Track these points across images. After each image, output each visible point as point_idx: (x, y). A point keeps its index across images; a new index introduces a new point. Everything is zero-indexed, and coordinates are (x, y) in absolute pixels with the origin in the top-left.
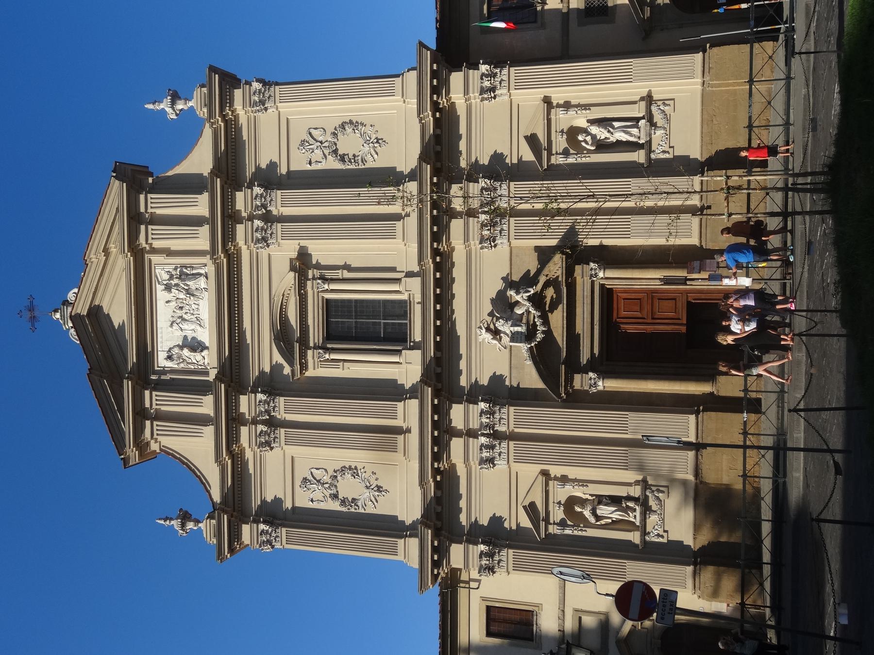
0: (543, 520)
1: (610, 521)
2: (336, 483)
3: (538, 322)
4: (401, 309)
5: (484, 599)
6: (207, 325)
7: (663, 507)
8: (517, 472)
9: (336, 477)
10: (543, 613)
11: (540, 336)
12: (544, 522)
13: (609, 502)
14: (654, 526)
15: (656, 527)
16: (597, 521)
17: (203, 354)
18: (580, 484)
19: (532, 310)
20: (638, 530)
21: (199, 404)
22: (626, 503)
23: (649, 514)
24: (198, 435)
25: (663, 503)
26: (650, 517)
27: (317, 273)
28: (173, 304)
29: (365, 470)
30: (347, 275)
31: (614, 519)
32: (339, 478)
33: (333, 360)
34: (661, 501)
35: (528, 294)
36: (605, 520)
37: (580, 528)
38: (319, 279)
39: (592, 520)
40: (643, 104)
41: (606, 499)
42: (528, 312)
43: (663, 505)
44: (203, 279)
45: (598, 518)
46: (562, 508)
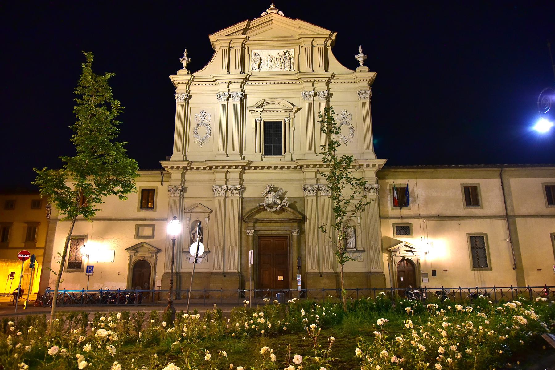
1: (193, 239)
2: (204, 125)
3: (275, 209)
4: (278, 152)
5: (157, 187)
6: (270, 71)
9: (207, 125)
10: (153, 212)
11: (268, 209)
17: (257, 69)
19: (279, 206)
21: (236, 67)
24: (223, 67)
27: (292, 117)
28: (278, 57)
29: (210, 138)
30: (292, 129)
32: (207, 127)
33: (256, 125)
35: (286, 205)
38: (290, 118)
39: (193, 232)
40: (362, 249)
42: (278, 205)
44: (289, 69)
45: (194, 234)
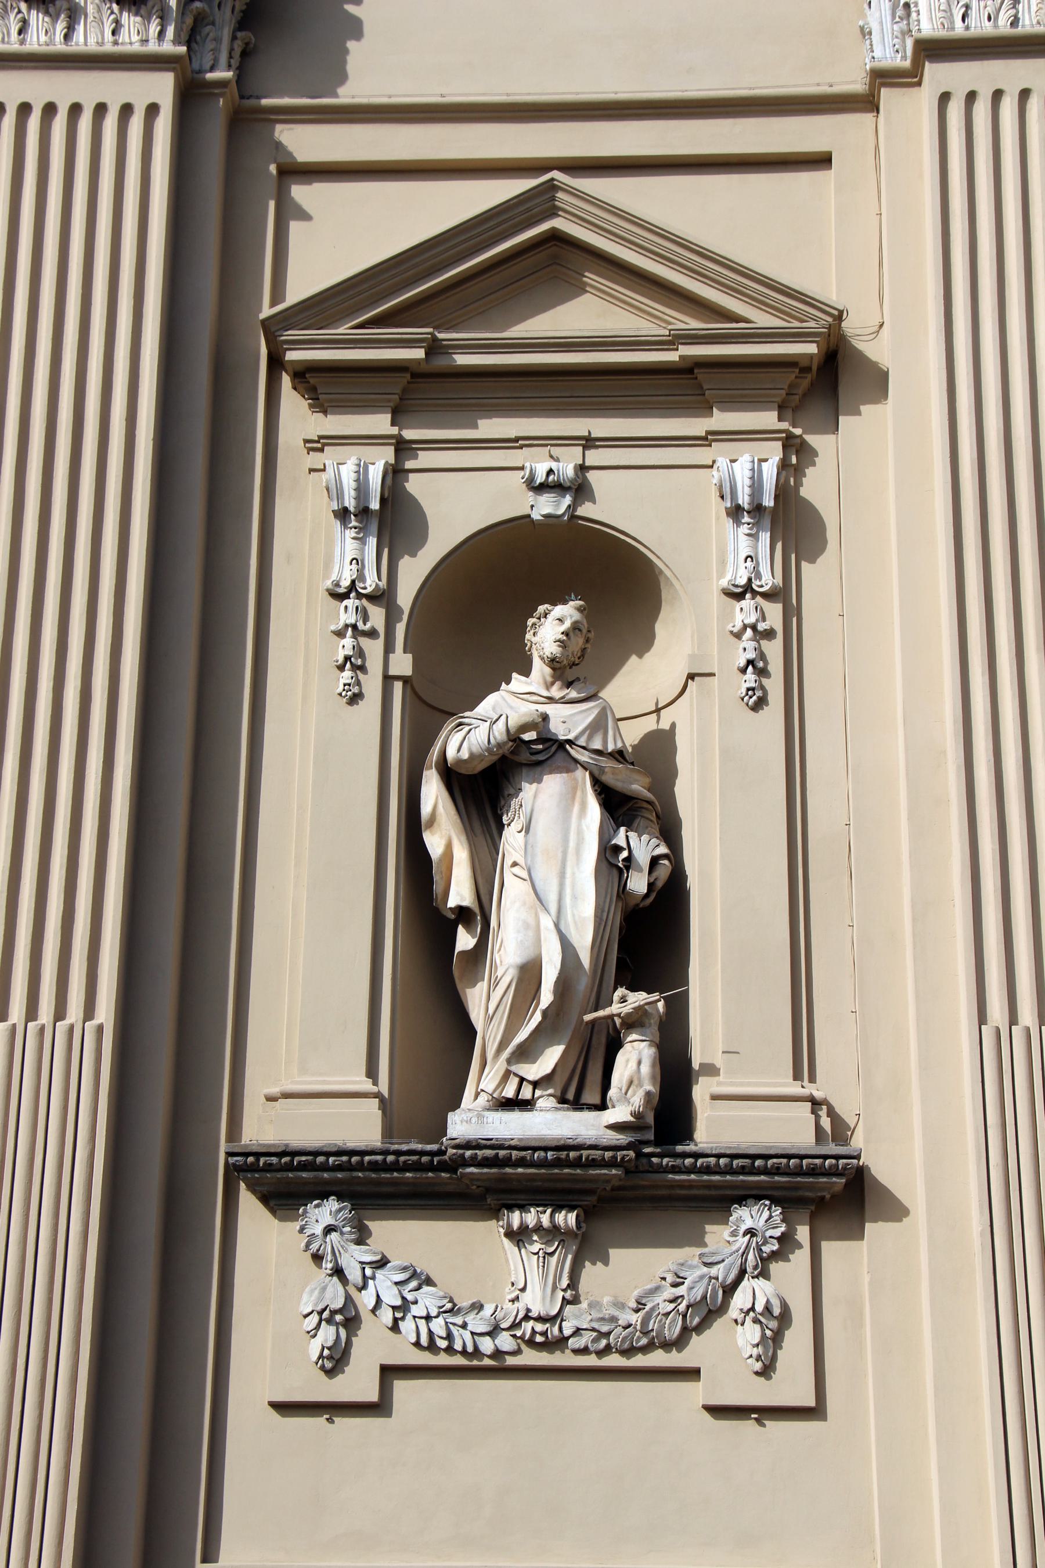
0: (434, 348)
7: (614, 1360)
8: (822, 161)
12: (419, 354)
13: (638, 884)
14: (429, 1282)
15: (427, 1301)
16: (450, 775)
18: (774, 649)
20: (388, 1132)
22: (635, 1021)
23: (553, 1233)
25: (658, 1359)
26: (519, 1236)
31: (465, 940)
34: (679, 1343)
36: (461, 855)
37: (374, 649)
41: (654, 861)
43: (639, 1361)
46: (546, 506)
